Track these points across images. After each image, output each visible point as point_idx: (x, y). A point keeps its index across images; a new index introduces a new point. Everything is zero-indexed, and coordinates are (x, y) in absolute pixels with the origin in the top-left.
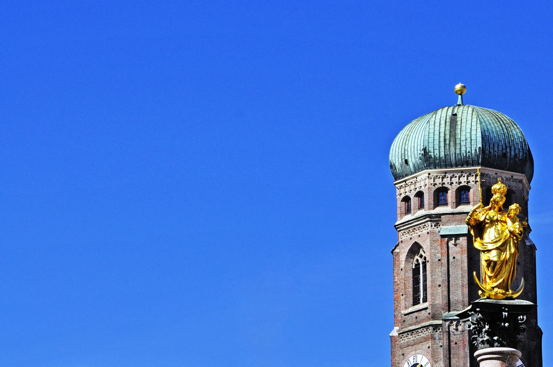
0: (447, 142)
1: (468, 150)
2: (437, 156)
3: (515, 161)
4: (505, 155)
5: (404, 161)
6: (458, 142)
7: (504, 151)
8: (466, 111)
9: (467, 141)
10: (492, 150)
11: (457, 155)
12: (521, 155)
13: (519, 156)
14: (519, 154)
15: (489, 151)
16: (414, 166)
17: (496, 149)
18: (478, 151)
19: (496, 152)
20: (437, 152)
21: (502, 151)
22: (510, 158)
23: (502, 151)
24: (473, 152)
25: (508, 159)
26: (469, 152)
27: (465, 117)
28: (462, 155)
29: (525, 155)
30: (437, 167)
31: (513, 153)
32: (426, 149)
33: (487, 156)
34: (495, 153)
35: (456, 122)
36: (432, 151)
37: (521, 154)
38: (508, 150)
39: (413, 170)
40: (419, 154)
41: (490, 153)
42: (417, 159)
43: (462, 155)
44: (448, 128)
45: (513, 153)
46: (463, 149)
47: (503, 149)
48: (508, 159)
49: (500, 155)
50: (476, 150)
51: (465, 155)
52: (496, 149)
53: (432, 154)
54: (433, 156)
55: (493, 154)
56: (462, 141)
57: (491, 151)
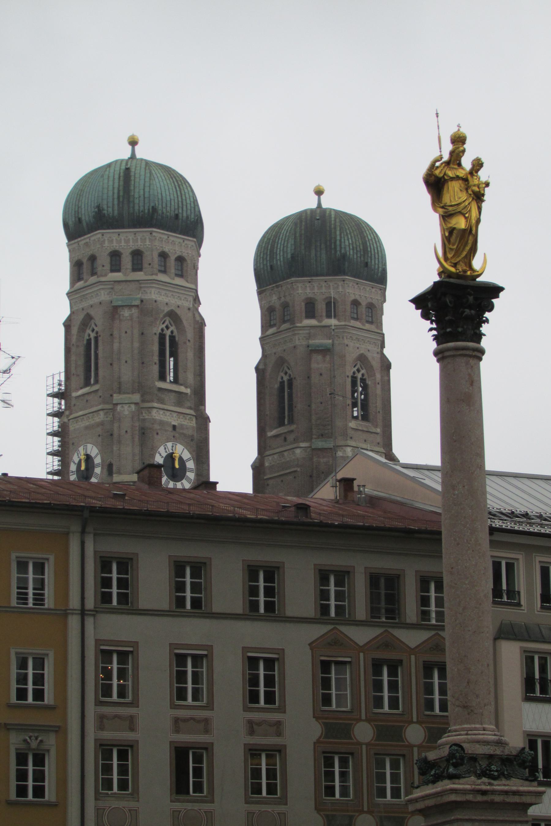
0: (121, 199)
1: (142, 208)
2: (111, 215)
4: (177, 216)
5: (77, 219)
6: (131, 199)
7: (176, 212)
10: (164, 210)
13: (191, 219)
15: (162, 211)
16: (87, 224)
18: (151, 210)
20: (110, 210)
21: (174, 211)
22: (182, 219)
23: (174, 211)
24: (146, 211)
25: (180, 221)
26: (142, 211)
29: (196, 218)
31: (185, 215)
33: (160, 217)
35: (130, 177)
37: (193, 216)
38: (180, 211)
41: (163, 213)
45: (185, 215)
46: (137, 207)
47: (175, 209)
48: (180, 221)
50: (149, 210)
52: (168, 209)
53: (105, 212)
54: (106, 215)
55: (166, 215)
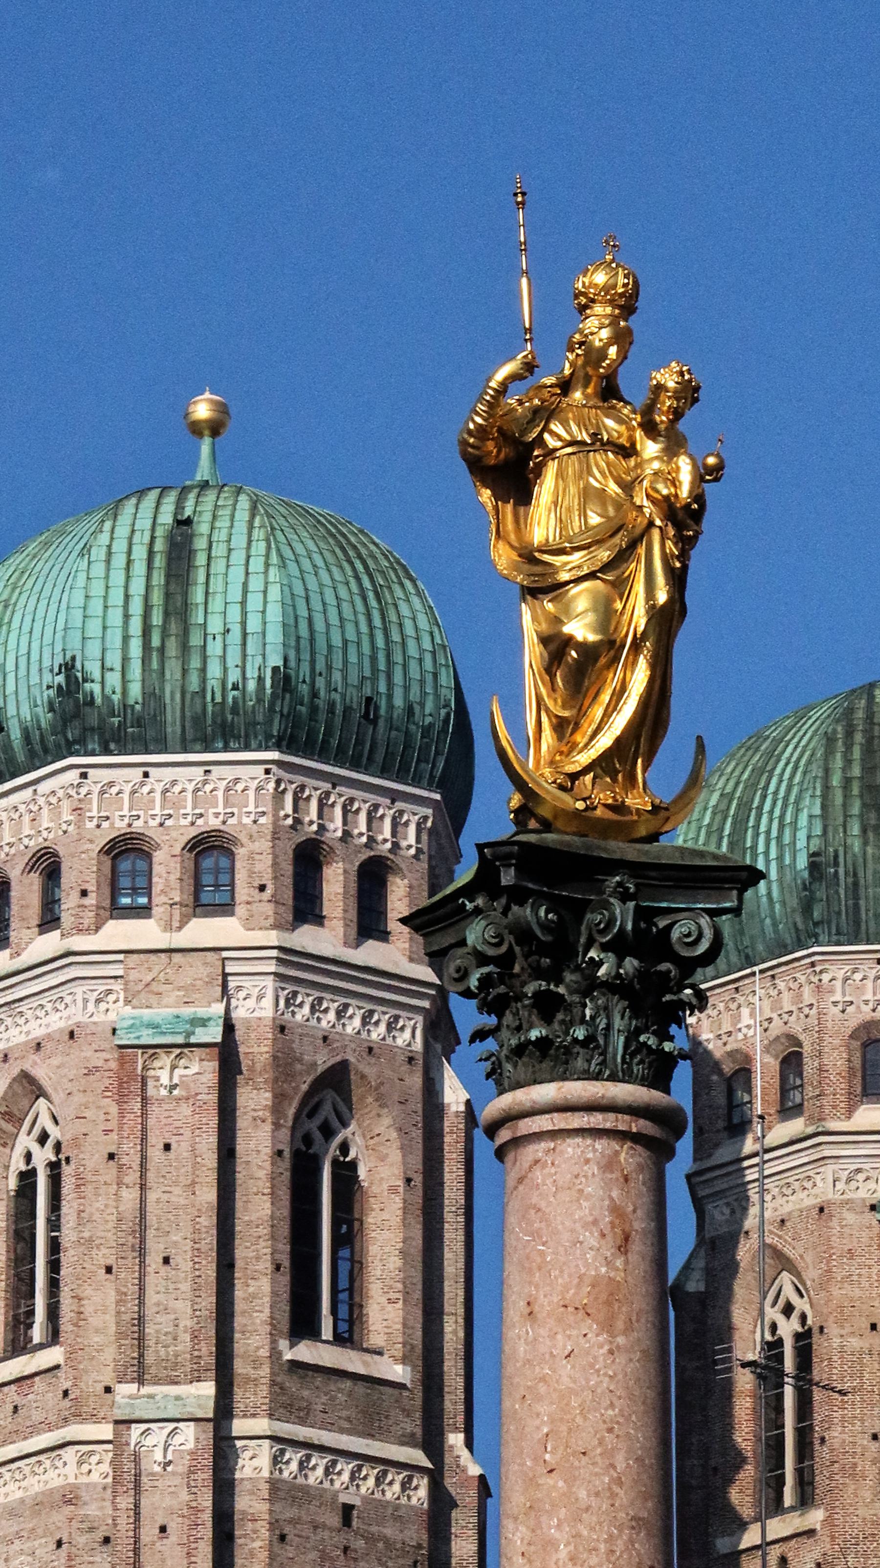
0: (156, 642)
1: (234, 676)
2: (116, 698)
3: (407, 733)
6: (195, 640)
7: (368, 691)
8: (227, 511)
9: (230, 638)
10: (320, 683)
11: (188, 697)
12: (427, 711)
14: (422, 705)
17: (337, 676)
19: (335, 690)
20: (114, 679)
24: (252, 685)
25: (381, 723)
26: (235, 687)
27: (223, 536)
28: (209, 698)
29: (443, 712)
30: (112, 746)
31: (398, 702)
32: (73, 666)
33: (303, 709)
34: (334, 695)
35: (191, 553)
36: (97, 675)
37: (429, 707)
38: (382, 688)
39: (21, 756)
40: (49, 687)
41: (314, 694)
42: (39, 710)
43: (209, 698)
44: (158, 578)
45: (398, 702)
46: (214, 670)
49: (351, 708)
50: (260, 680)
51: (218, 699)
52: (337, 676)
53: (96, 688)
54: (98, 700)
56: (210, 638)
57: (317, 685)
